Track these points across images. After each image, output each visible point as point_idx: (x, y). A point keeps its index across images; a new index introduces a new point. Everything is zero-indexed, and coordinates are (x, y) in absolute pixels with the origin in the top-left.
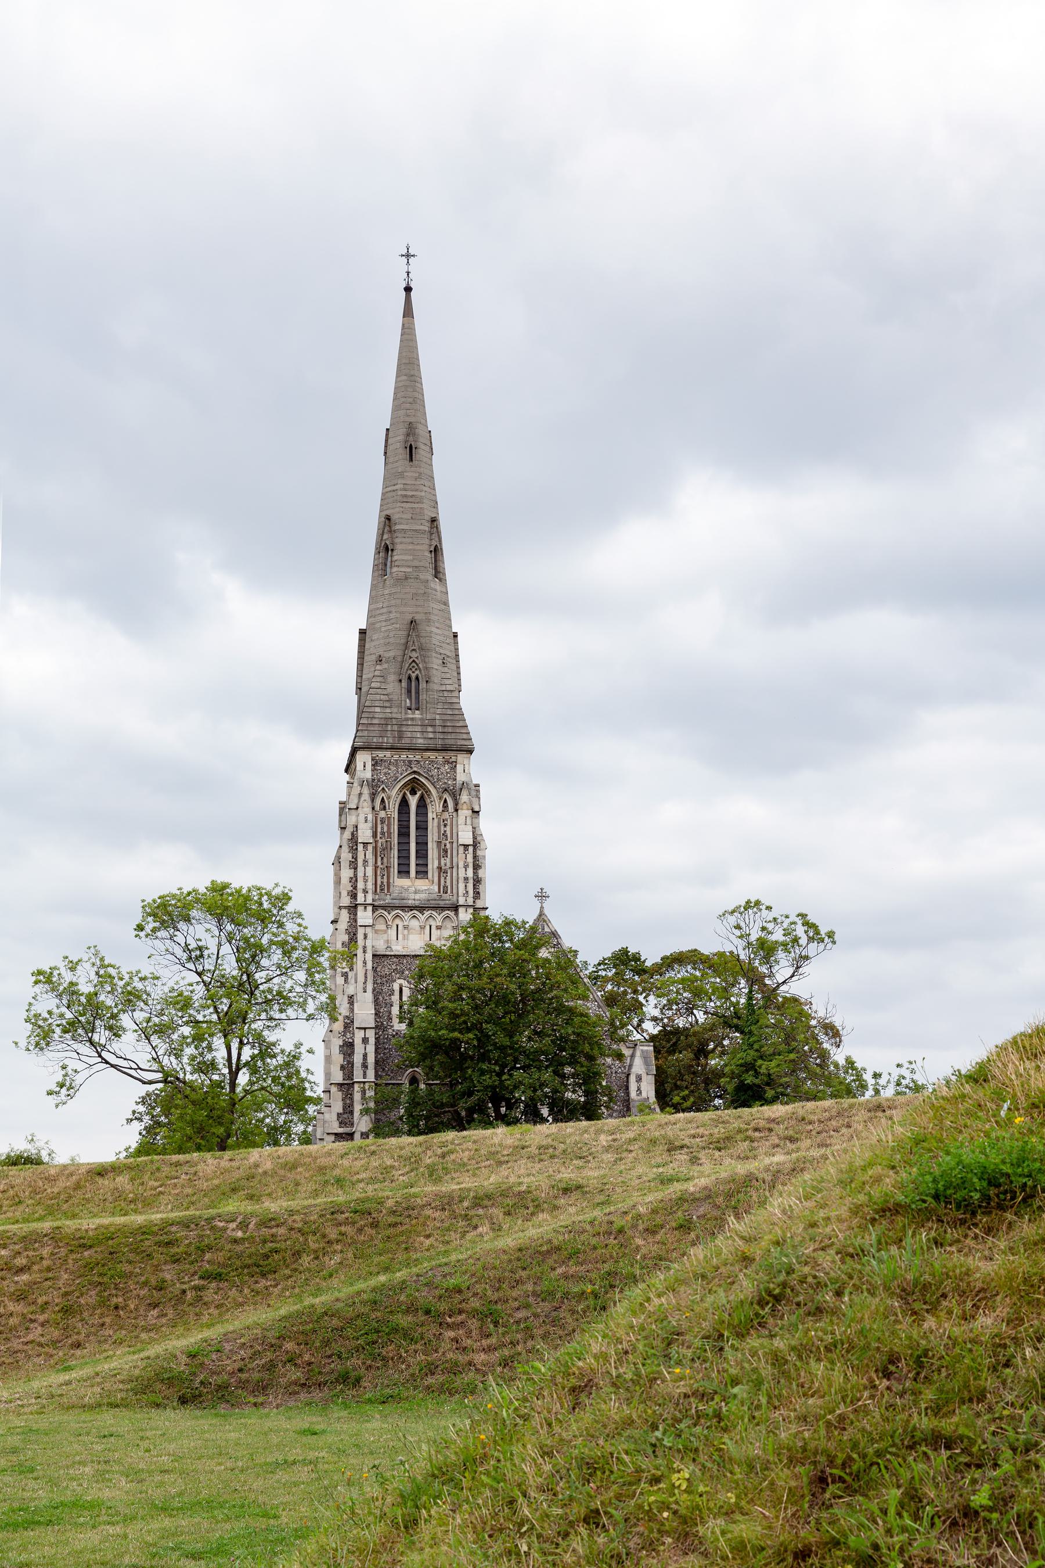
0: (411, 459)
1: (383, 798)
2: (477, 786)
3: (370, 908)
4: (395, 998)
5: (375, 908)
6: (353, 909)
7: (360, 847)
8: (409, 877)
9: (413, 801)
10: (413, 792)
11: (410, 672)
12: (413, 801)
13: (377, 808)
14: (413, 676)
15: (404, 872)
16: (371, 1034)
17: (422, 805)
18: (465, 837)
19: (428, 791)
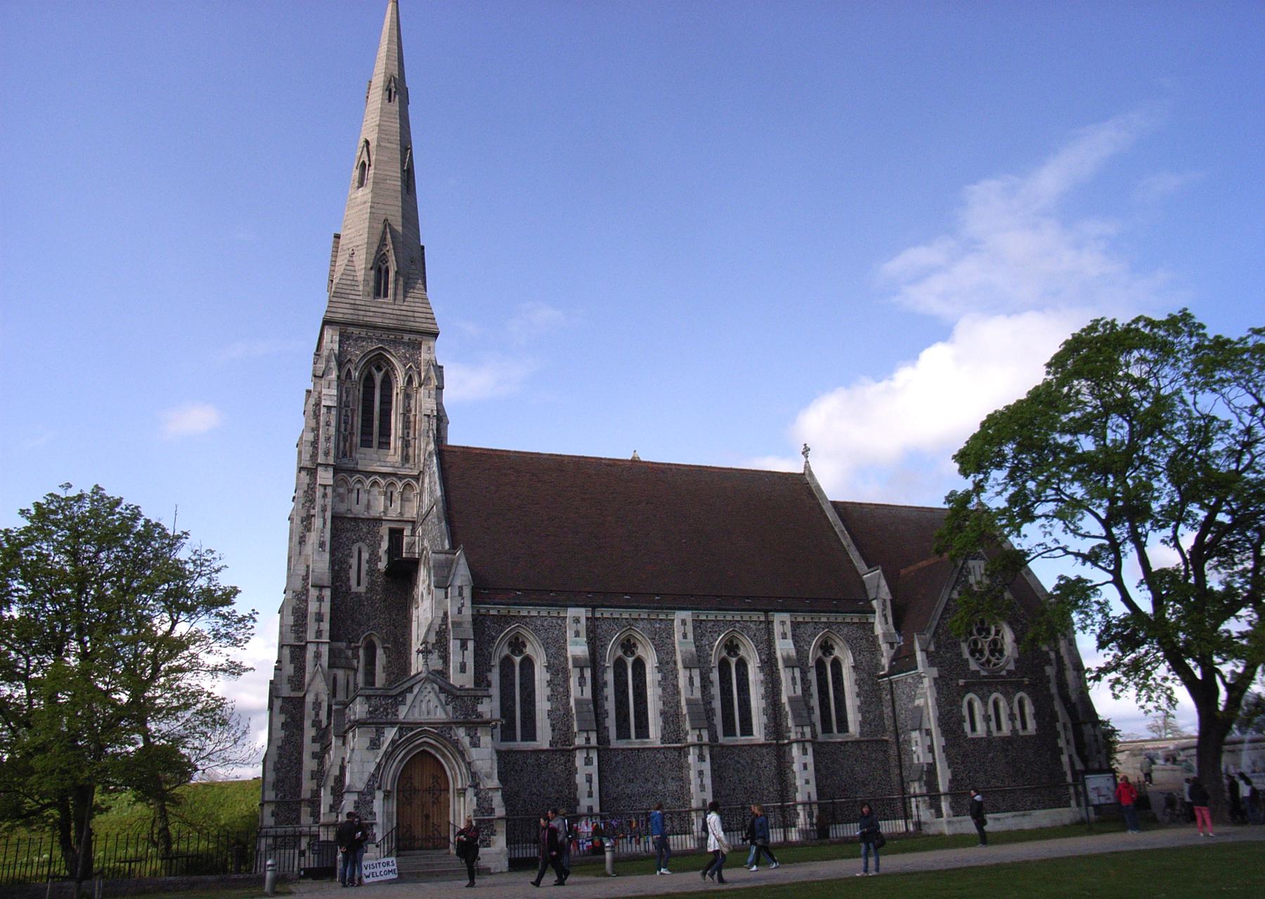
0: (390, 101)
1: (349, 369)
2: (442, 367)
3: (331, 471)
4: (354, 562)
5: (337, 470)
6: (312, 472)
7: (323, 410)
8: (371, 447)
9: (378, 377)
10: (379, 369)
11: (380, 263)
12: (378, 377)
13: (343, 377)
14: (384, 267)
15: (367, 443)
16: (327, 593)
17: (387, 384)
18: (428, 405)
19: (393, 369)
